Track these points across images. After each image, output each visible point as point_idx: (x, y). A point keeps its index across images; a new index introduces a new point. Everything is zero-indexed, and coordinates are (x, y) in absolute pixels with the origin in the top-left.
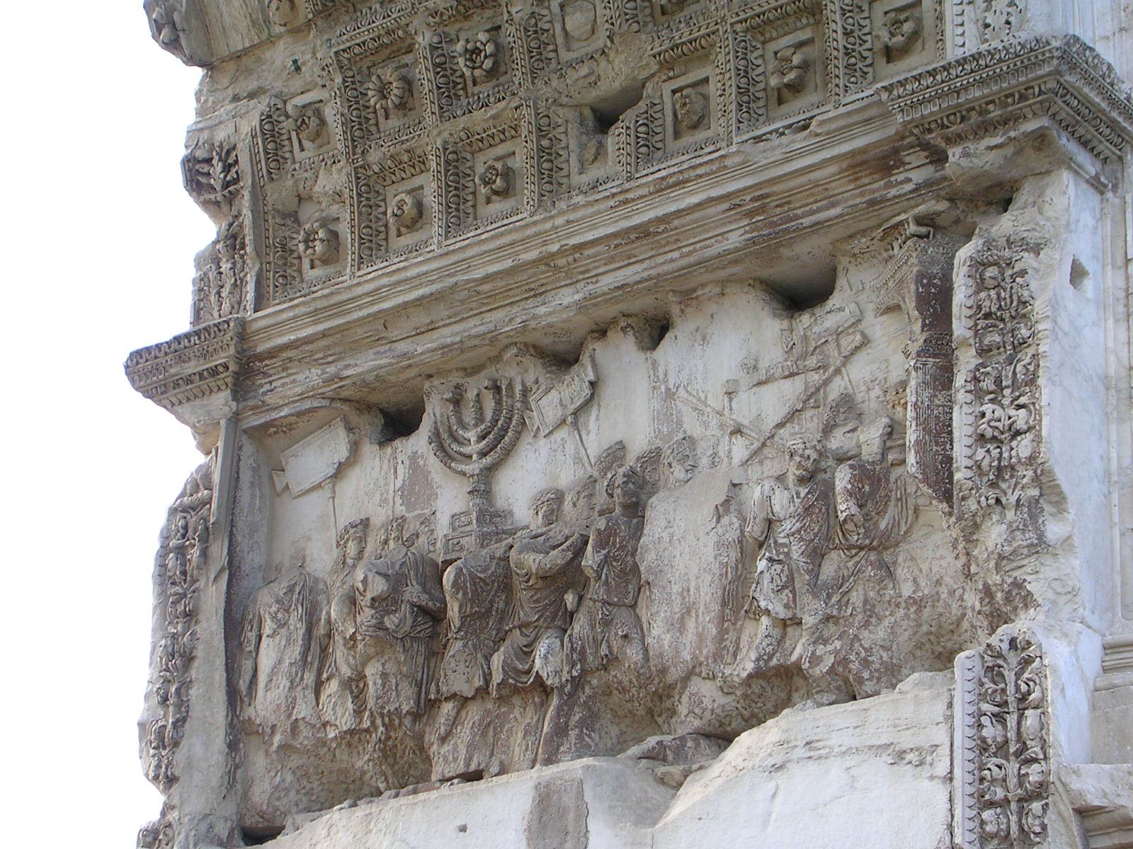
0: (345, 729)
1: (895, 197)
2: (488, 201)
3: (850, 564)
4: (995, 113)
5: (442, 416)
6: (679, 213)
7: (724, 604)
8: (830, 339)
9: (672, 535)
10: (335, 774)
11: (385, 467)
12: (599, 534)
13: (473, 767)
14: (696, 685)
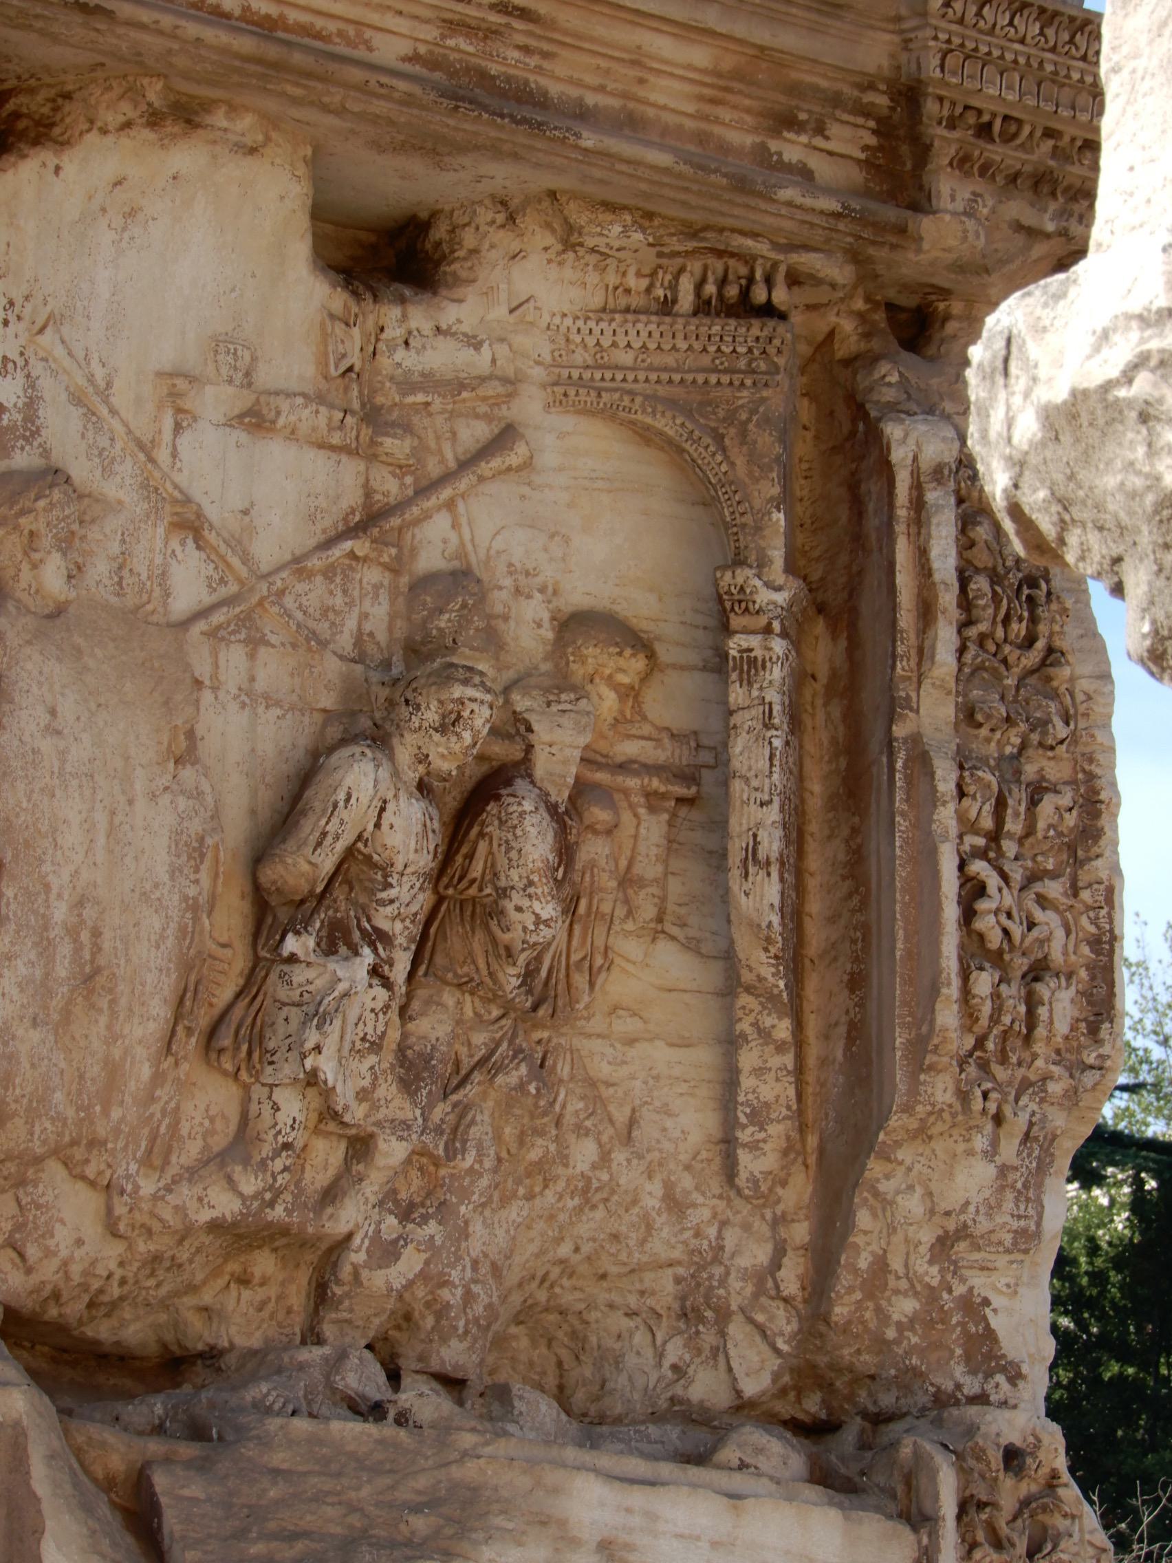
1: (789, 204)
8: (437, 403)
9: (63, 754)
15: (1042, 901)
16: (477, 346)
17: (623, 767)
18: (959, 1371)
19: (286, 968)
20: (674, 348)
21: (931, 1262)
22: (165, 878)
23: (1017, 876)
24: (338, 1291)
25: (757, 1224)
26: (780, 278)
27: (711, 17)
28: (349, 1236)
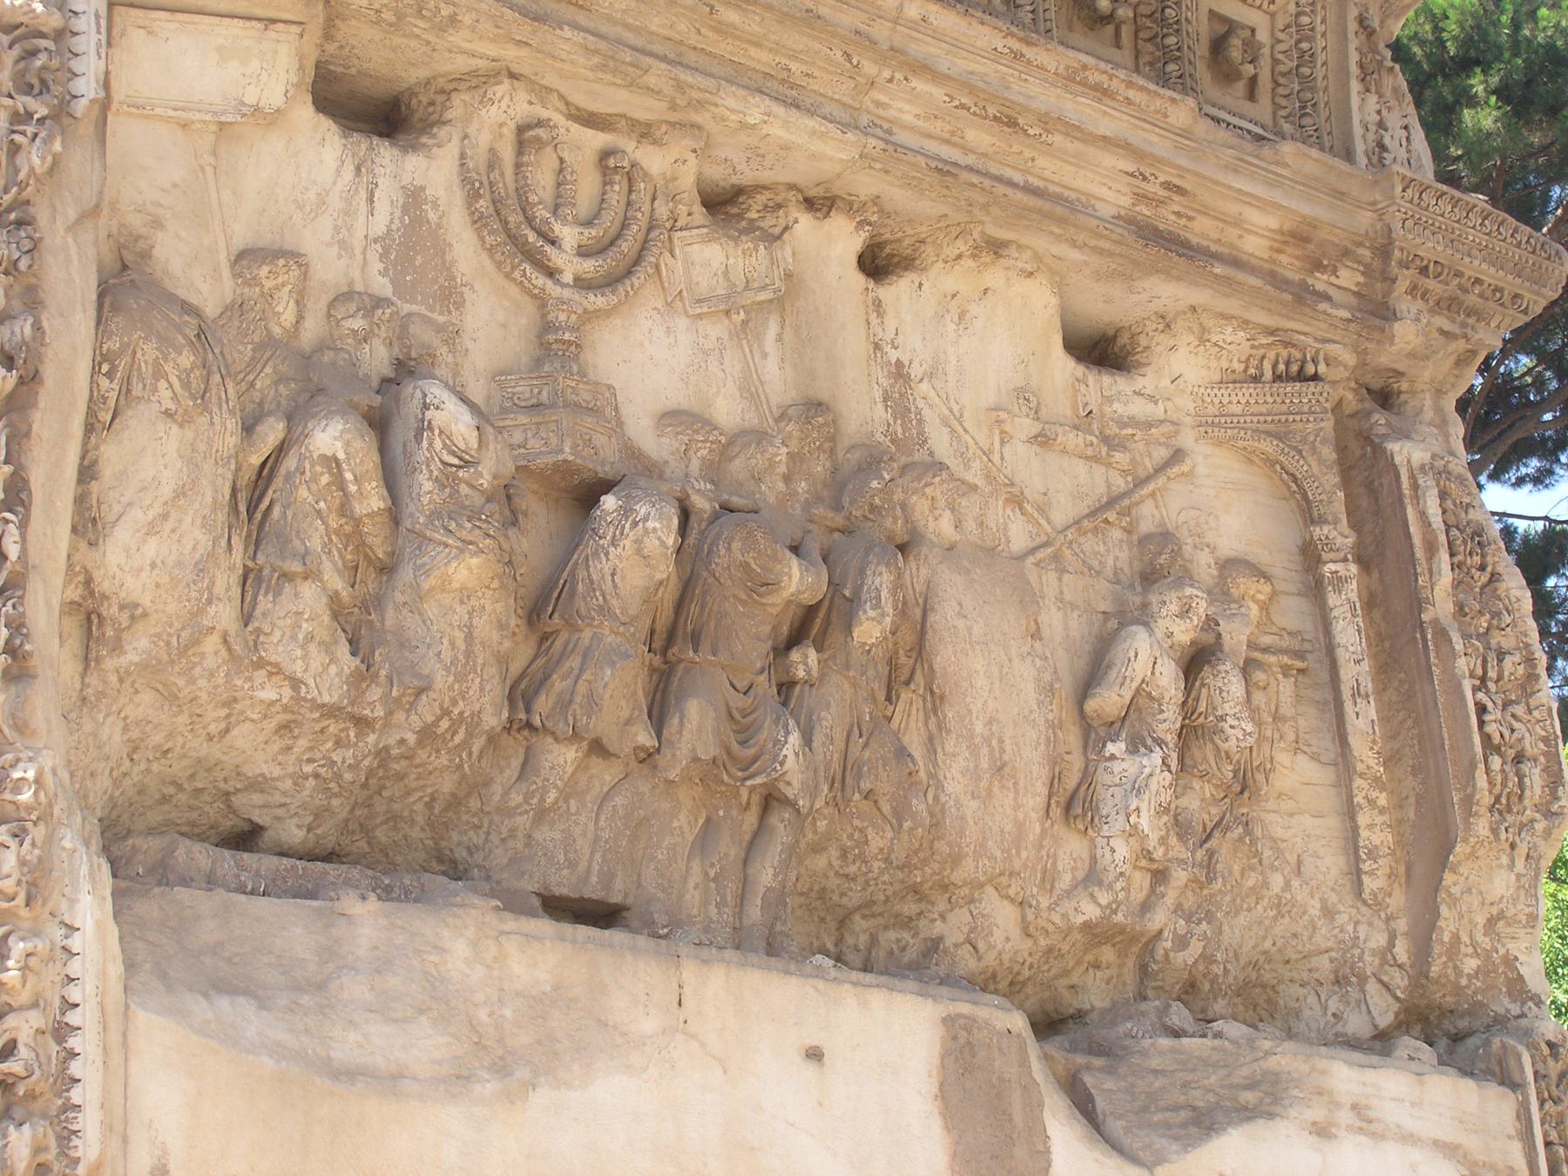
0: (326, 699)
1: (1324, 312)
3: (1214, 810)
4: (1472, 299)
6: (1074, 131)
9: (969, 629)
10: (185, 763)
11: (348, 172)
15: (1513, 716)
16: (1156, 403)
17: (1266, 650)
18: (1506, 1001)
19: (1108, 764)
20: (1265, 402)
21: (1485, 935)
23: (1499, 702)
24: (1155, 967)
25: (1376, 922)
26: (1321, 358)
28: (1161, 932)
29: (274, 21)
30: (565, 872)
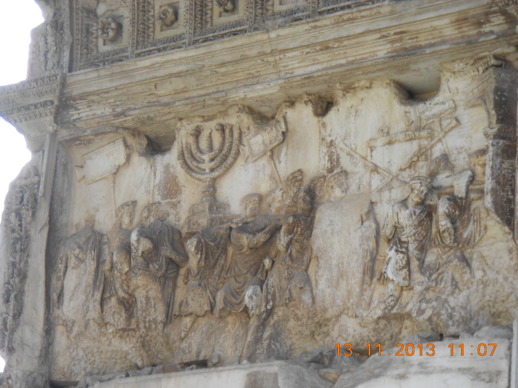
0: (120, 327)
1: (483, 41)
2: (220, 15)
3: (444, 257)
5: (187, 143)
6: (348, 38)
7: (364, 273)
9: (333, 230)
11: (149, 170)
12: (289, 226)
13: (201, 358)
14: (345, 320)
22: (358, 247)
27: (442, 12)
29: (115, 141)
30: (188, 355)
